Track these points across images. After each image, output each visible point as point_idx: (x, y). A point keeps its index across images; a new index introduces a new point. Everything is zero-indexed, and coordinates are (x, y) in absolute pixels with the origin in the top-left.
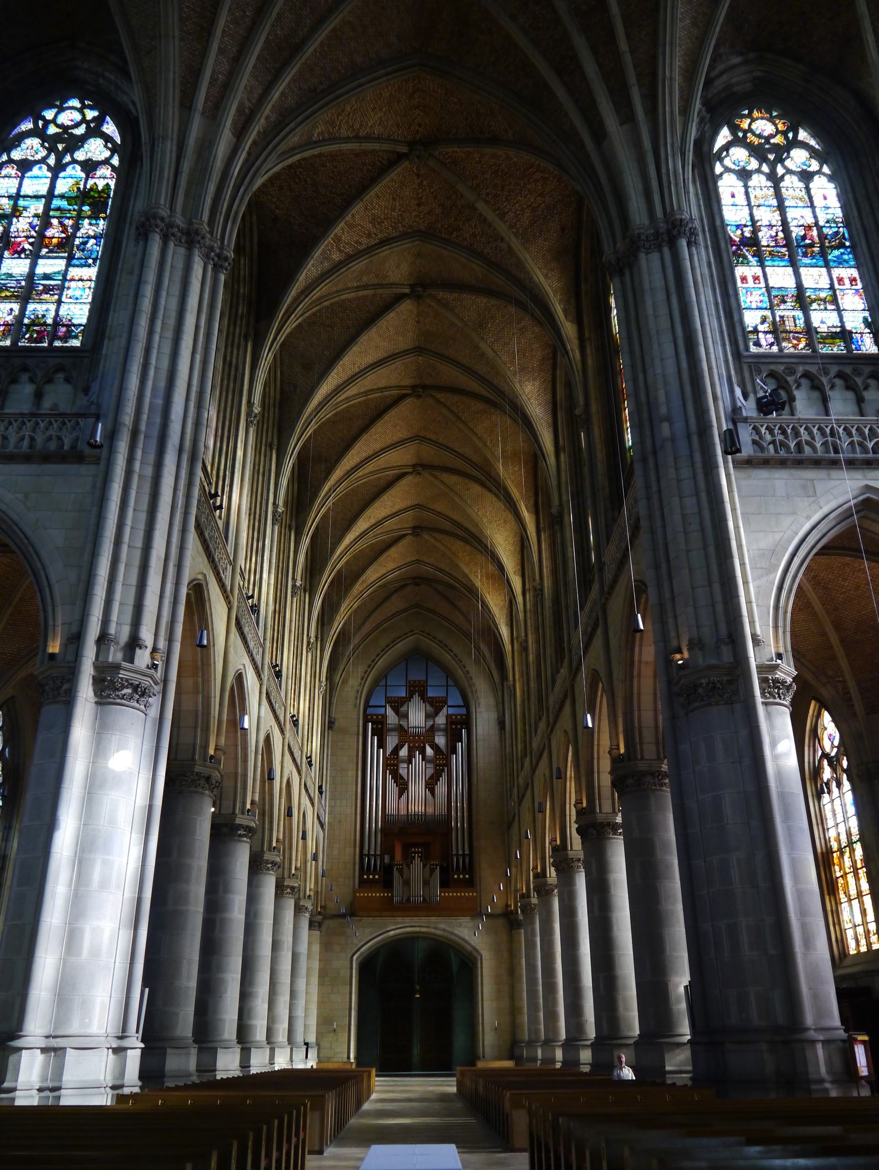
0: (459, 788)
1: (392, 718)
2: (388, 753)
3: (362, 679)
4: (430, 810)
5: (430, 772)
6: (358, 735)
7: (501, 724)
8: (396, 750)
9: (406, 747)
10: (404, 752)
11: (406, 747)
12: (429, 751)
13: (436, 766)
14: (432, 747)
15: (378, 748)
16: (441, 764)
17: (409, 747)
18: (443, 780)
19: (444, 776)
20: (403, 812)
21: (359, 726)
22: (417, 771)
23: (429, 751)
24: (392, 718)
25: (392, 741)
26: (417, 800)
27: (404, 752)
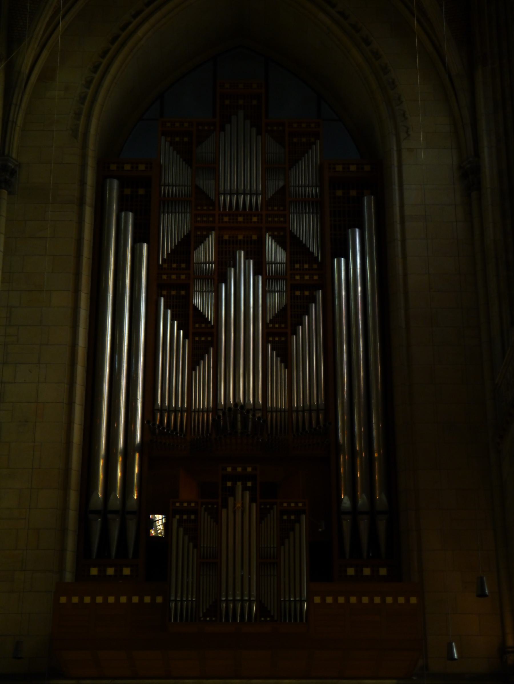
0: (355, 352)
1: (175, 176)
2: (164, 254)
3: (96, 68)
4: (278, 401)
5: (277, 300)
6: (81, 203)
7: (469, 176)
8: (185, 248)
9: (211, 240)
10: (206, 253)
11: (211, 240)
12: (274, 252)
13: (292, 288)
14: (281, 242)
15: (137, 240)
16: (306, 283)
17: (219, 242)
18: (311, 326)
19: (316, 310)
20: (203, 400)
21: (82, 183)
22: (244, 299)
23: (274, 252)
24: (175, 176)
25: (173, 227)
26: (242, 381)
27: (206, 253)
